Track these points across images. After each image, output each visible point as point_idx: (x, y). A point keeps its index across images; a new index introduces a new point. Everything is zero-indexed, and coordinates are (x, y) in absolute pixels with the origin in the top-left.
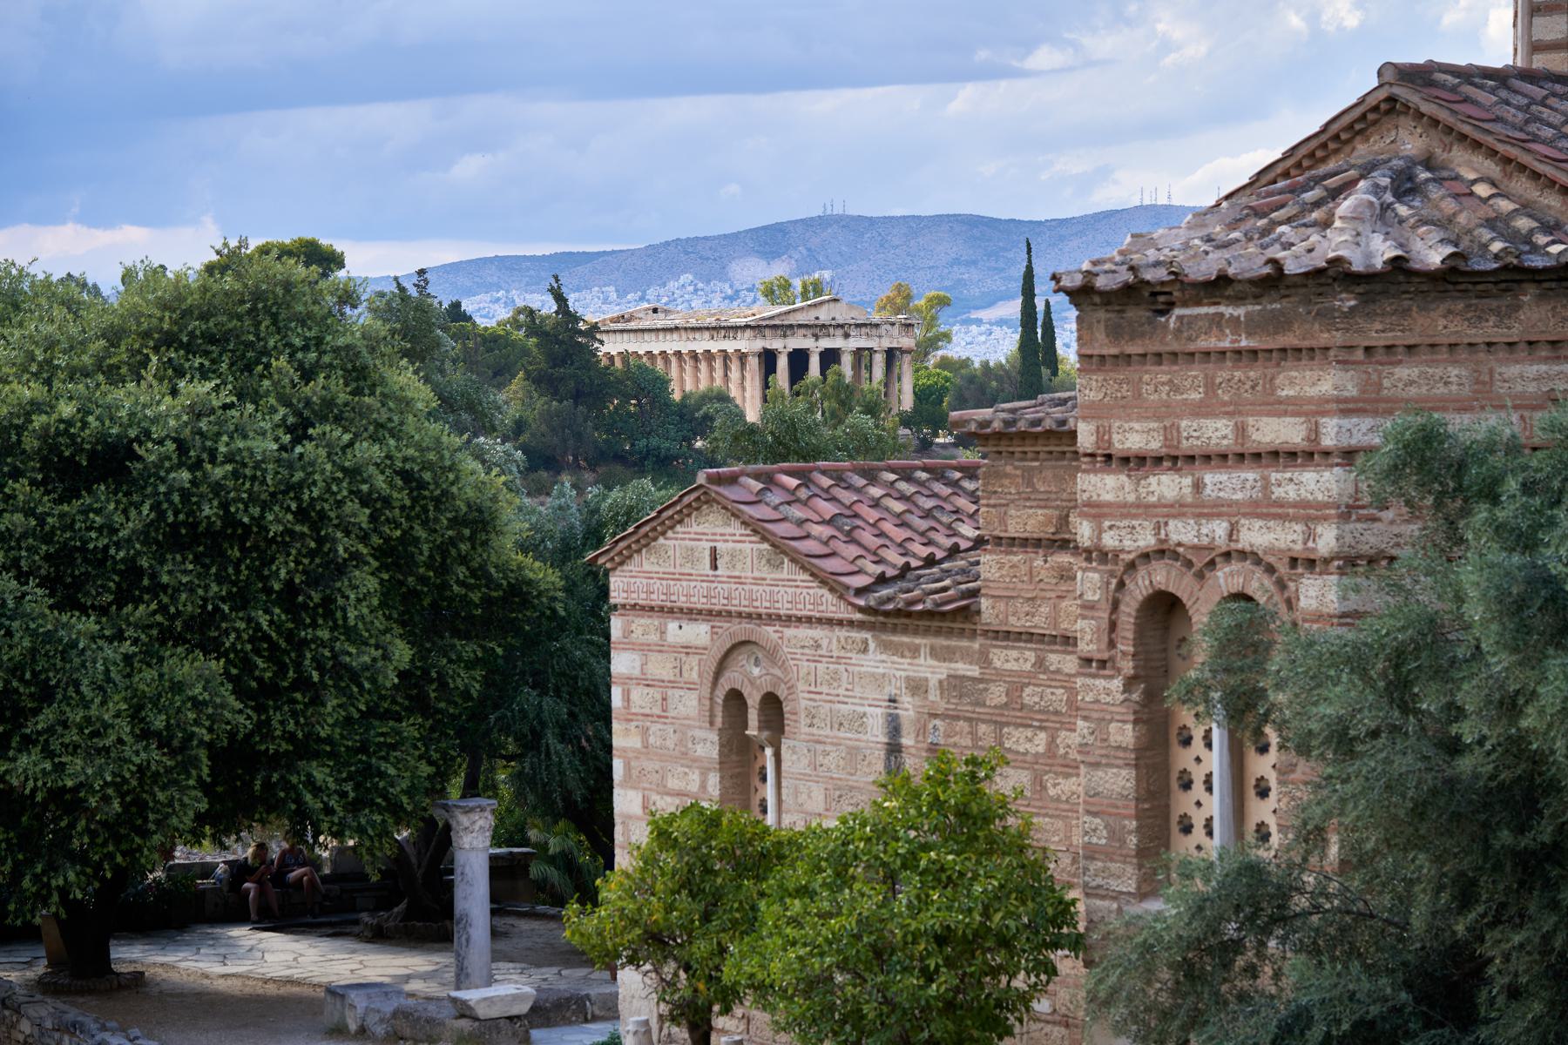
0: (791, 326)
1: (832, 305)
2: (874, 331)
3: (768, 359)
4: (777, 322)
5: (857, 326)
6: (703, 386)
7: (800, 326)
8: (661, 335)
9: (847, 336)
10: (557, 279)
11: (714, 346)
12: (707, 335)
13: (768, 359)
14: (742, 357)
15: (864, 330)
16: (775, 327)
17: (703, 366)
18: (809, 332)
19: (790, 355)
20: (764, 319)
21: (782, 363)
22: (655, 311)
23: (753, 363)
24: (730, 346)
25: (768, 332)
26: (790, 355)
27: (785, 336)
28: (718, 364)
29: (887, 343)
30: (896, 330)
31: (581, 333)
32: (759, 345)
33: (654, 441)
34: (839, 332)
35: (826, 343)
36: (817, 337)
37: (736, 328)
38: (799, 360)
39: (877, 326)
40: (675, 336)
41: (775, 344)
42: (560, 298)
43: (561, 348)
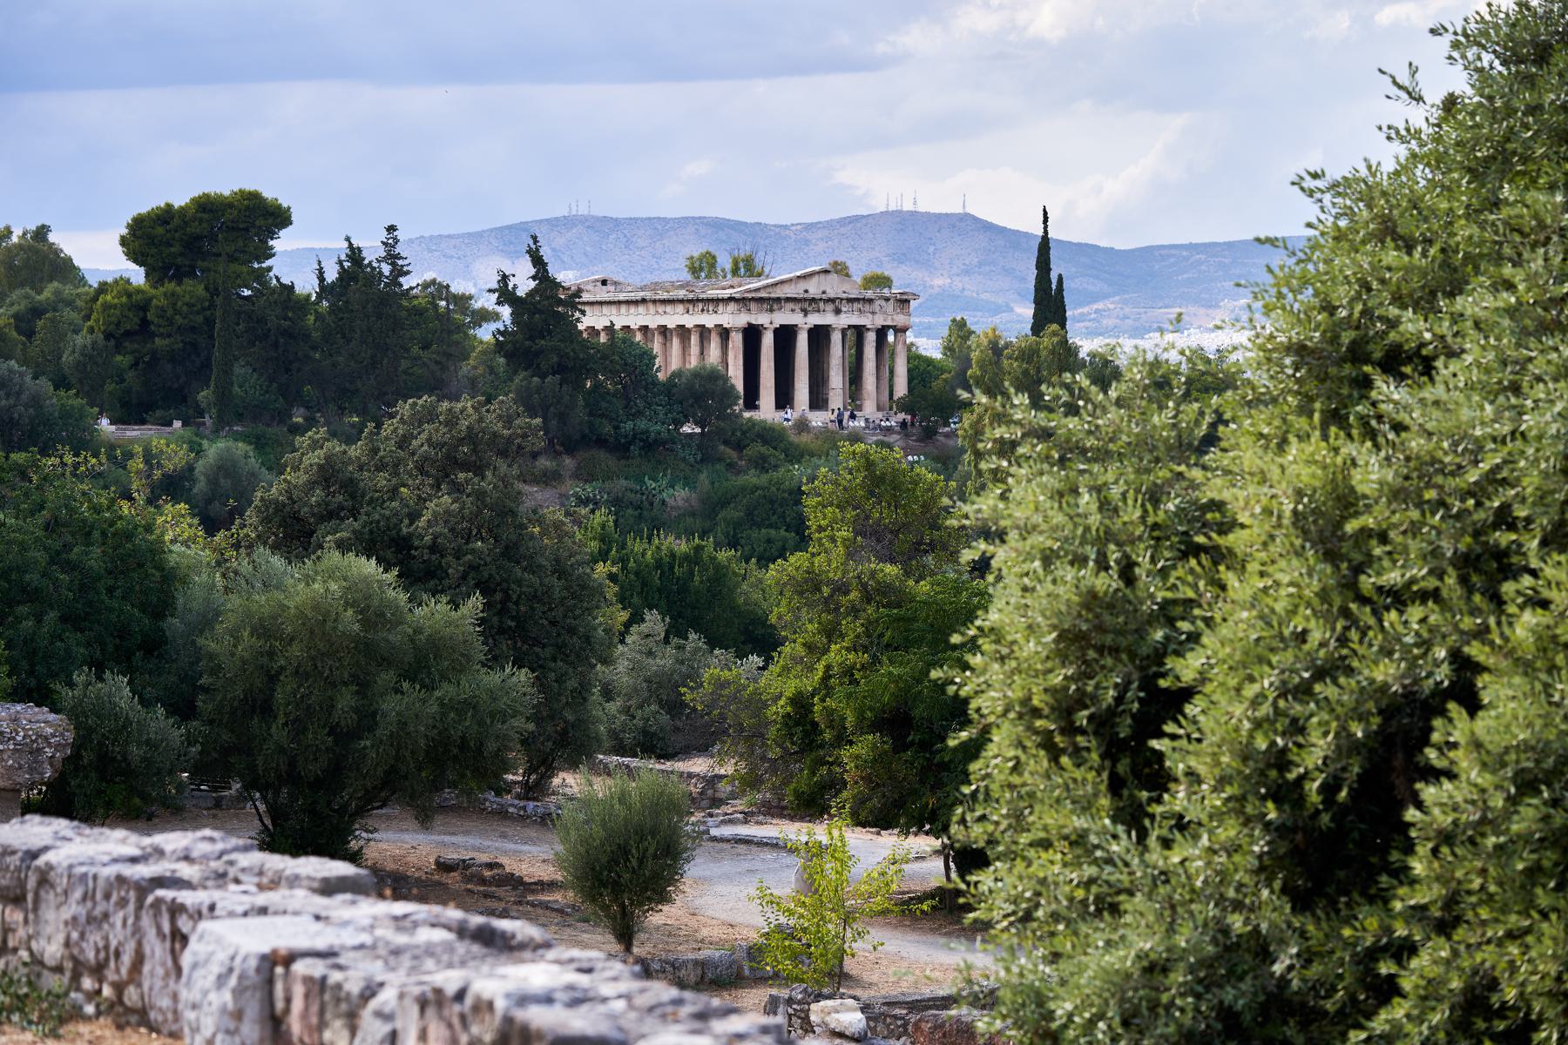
0: (778, 300)
1: (822, 276)
2: (867, 307)
3: (752, 335)
4: (763, 294)
5: (850, 300)
6: (693, 362)
7: (788, 300)
8: (623, 308)
9: (838, 311)
10: (535, 239)
11: (690, 321)
12: (680, 308)
13: (752, 335)
14: (724, 333)
15: (856, 305)
16: (761, 300)
17: (676, 342)
18: (797, 307)
19: (776, 331)
20: (750, 291)
21: (768, 341)
22: (604, 282)
23: (737, 340)
24: (709, 320)
25: (753, 306)
26: (776, 331)
27: (771, 310)
28: (694, 339)
29: (880, 321)
30: (890, 306)
31: (560, 302)
32: (743, 319)
33: (642, 424)
34: (830, 307)
35: (815, 319)
36: (805, 312)
37: (717, 301)
38: (785, 336)
39: (870, 301)
40: (641, 309)
41: (761, 319)
42: (538, 261)
43: (544, 311)
